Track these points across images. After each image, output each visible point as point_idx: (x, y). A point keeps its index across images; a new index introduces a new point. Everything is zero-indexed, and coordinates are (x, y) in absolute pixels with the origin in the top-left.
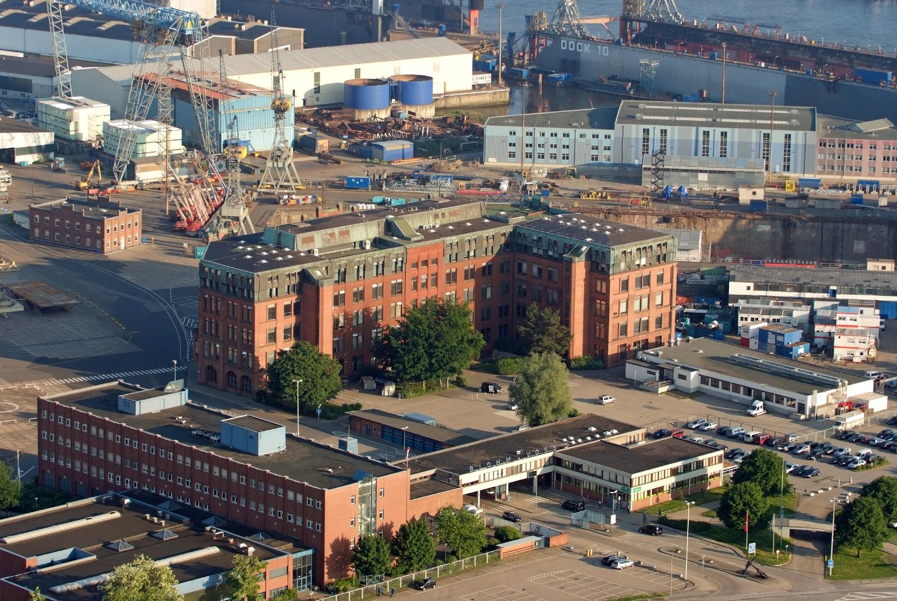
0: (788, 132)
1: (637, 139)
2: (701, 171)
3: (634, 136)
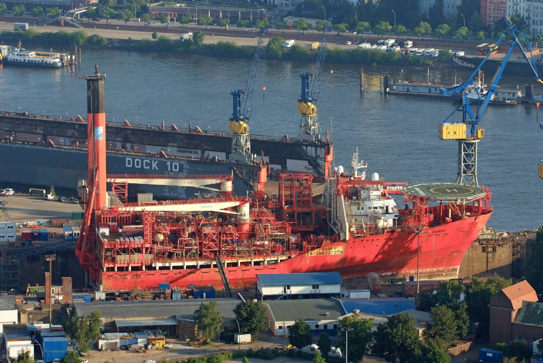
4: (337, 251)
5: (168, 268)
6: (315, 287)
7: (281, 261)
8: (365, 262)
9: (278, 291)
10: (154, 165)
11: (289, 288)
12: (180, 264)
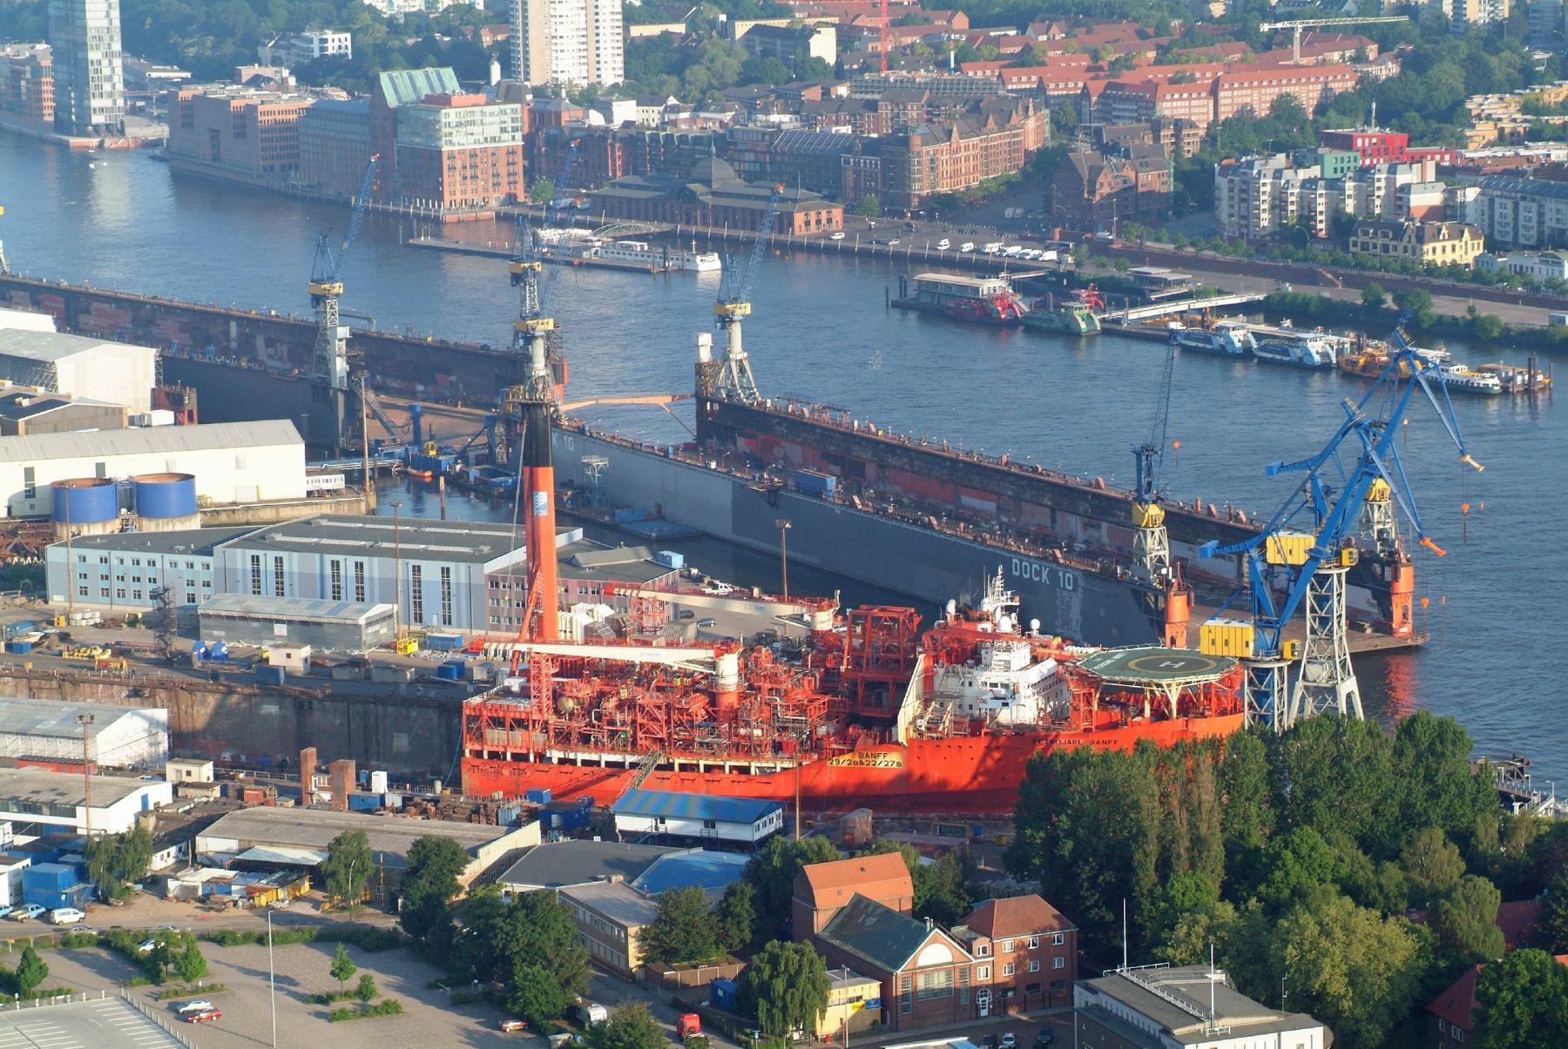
0: (446, 564)
1: (244, 571)
2: (278, 621)
3: (239, 566)
4: (889, 762)
5: (573, 762)
6: (710, 824)
7: (784, 769)
8: (951, 787)
9: (643, 824)
10: (1044, 576)
11: (663, 822)
12: (594, 757)
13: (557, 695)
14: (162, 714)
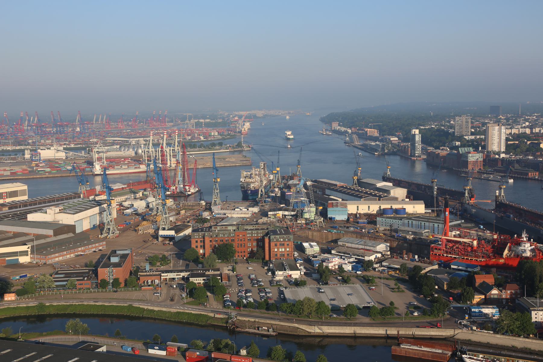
4: (502, 261)
6: (467, 268)
9: (455, 267)
13: (446, 245)
14: (388, 244)
